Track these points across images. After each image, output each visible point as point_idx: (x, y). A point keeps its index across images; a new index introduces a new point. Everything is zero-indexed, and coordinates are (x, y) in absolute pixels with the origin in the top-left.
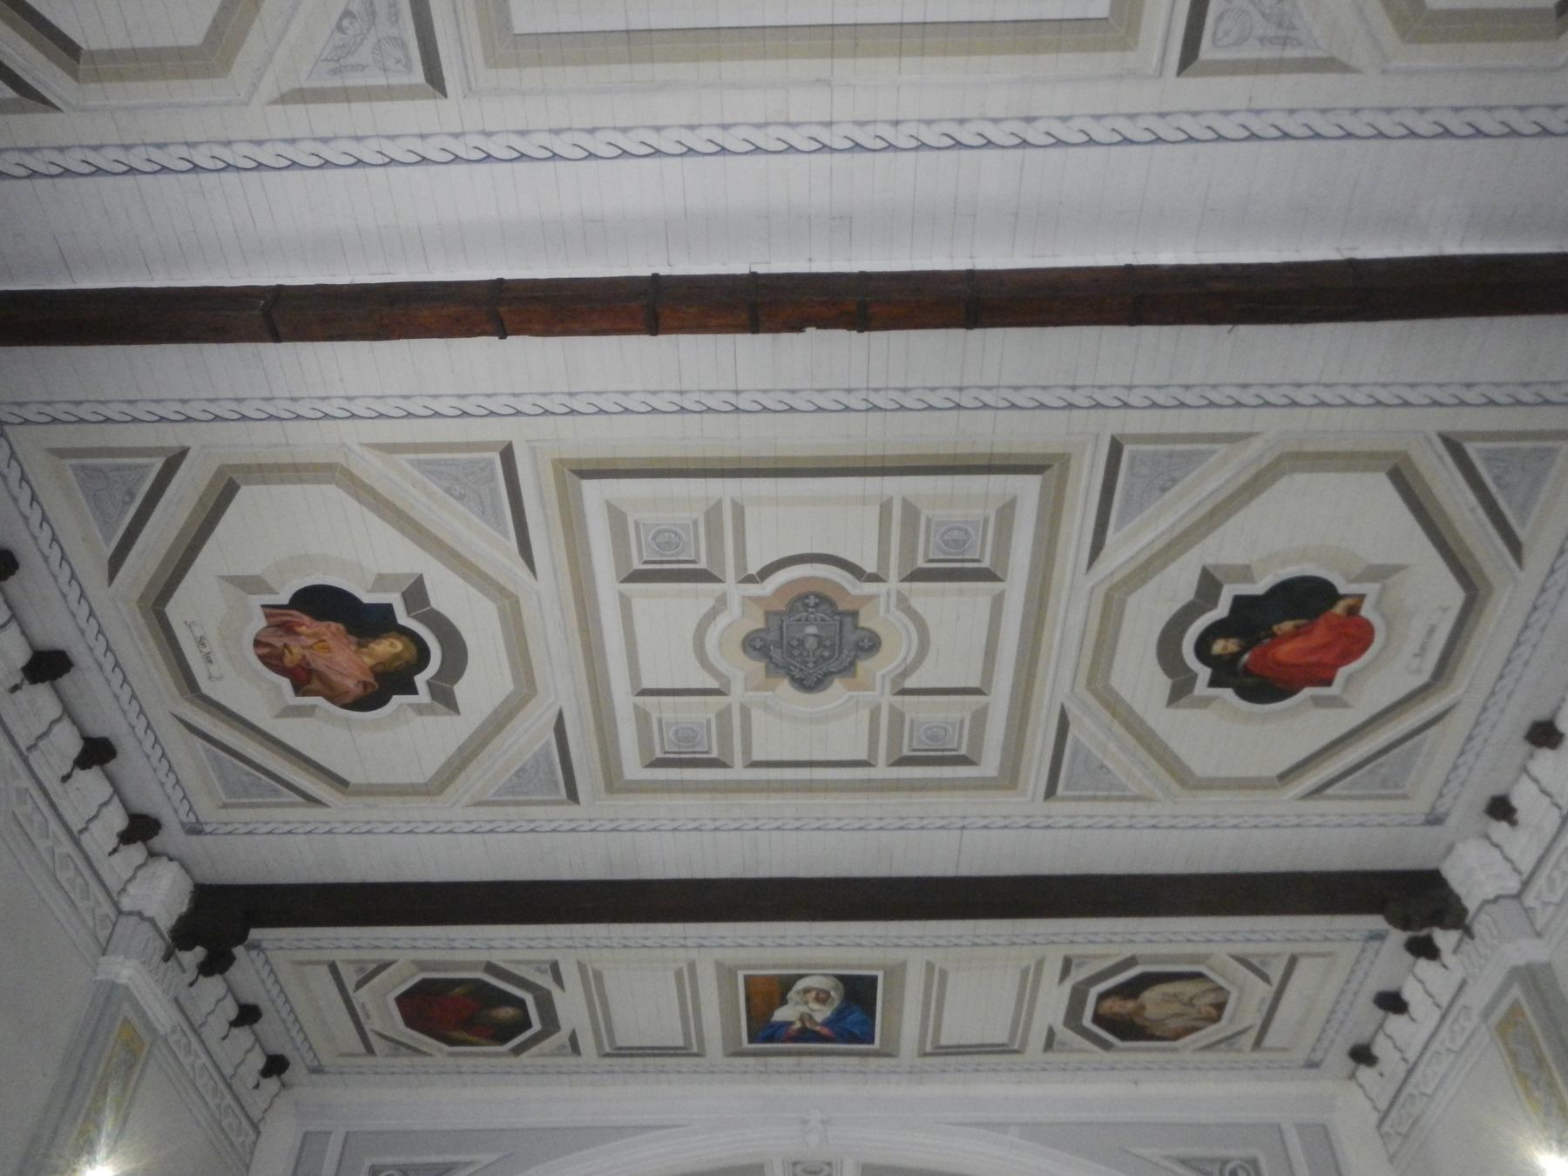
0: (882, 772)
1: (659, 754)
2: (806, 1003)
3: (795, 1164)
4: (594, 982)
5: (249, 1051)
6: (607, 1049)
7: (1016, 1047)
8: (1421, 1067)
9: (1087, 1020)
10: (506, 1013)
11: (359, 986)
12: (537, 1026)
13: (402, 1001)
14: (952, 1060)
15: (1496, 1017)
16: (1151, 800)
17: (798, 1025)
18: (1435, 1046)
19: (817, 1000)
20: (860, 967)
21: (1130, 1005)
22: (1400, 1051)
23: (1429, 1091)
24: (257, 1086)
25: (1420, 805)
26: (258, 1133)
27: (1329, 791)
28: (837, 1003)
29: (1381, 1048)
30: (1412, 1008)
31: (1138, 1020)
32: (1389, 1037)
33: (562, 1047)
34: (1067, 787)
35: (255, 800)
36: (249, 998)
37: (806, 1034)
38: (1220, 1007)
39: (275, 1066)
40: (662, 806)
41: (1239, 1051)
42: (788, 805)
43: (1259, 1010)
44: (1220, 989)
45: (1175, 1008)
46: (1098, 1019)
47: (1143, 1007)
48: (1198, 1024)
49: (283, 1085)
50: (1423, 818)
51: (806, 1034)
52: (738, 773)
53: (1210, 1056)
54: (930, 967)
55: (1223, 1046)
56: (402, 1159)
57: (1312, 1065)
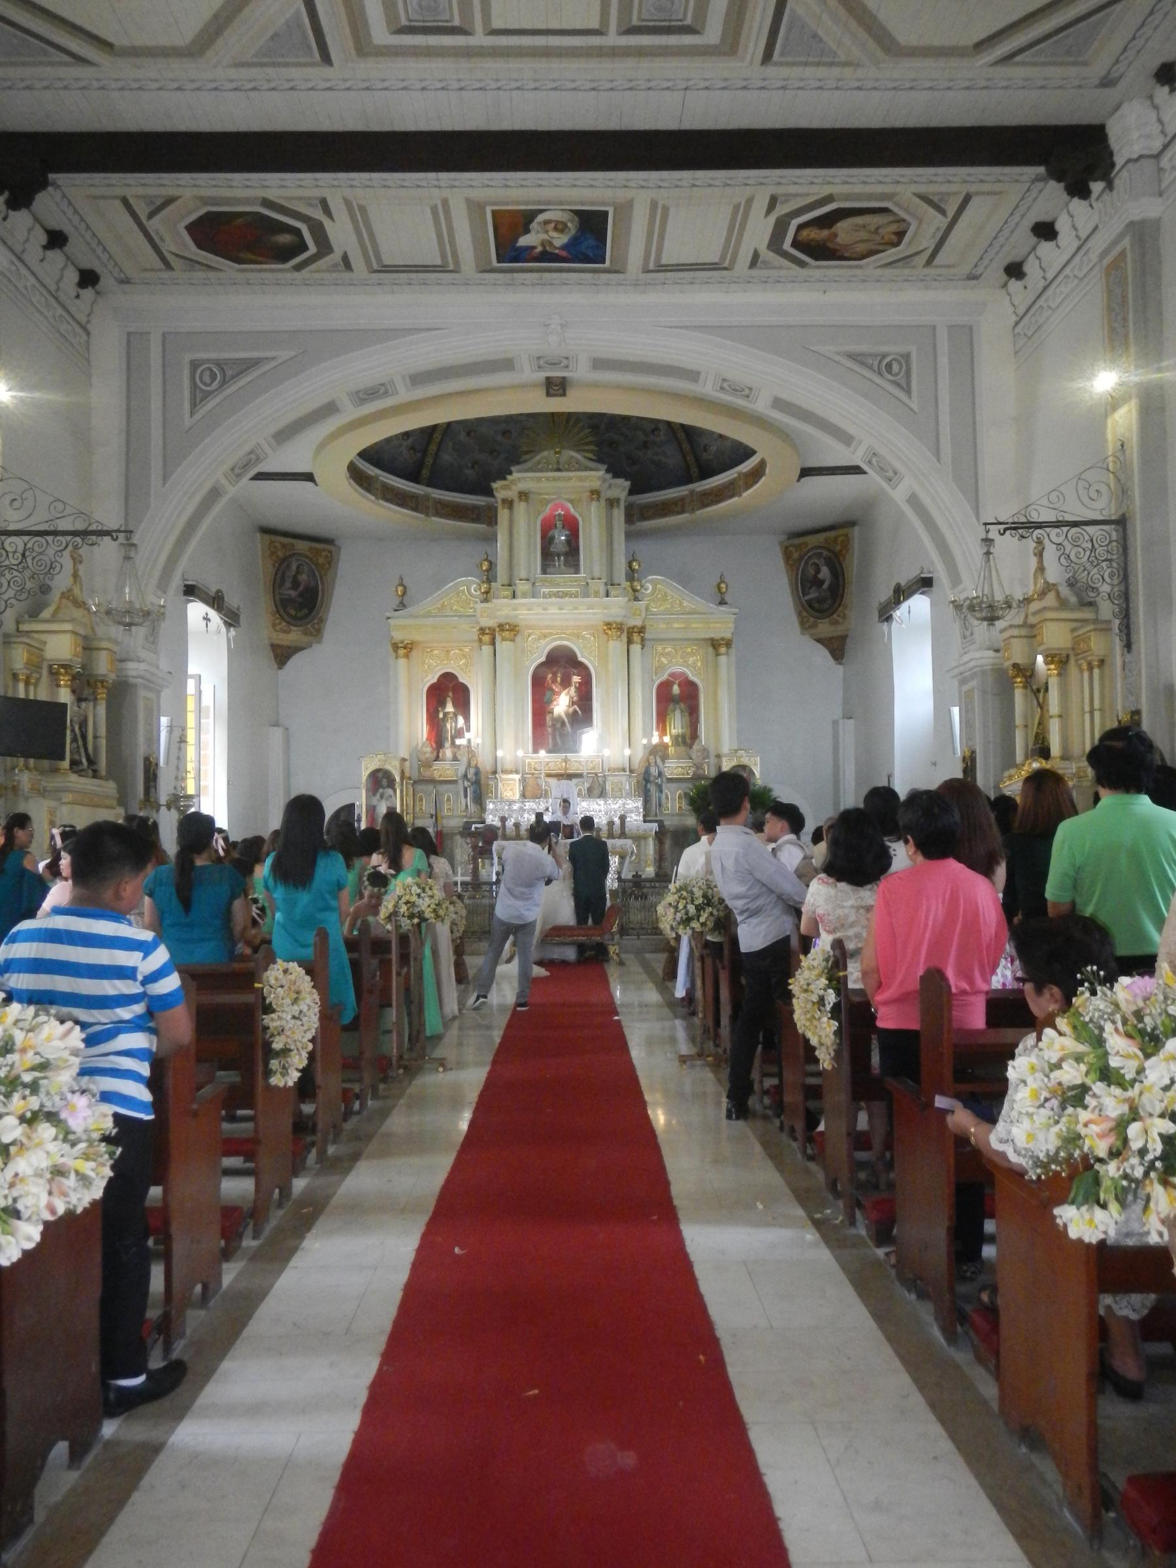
0: (613, 39)
1: (404, 22)
2: (547, 232)
3: (539, 358)
4: (359, 215)
5: (63, 269)
6: (375, 266)
7: (726, 264)
8: (1054, 286)
9: (787, 245)
10: (285, 239)
11: (151, 215)
12: (312, 249)
13: (190, 228)
14: (669, 274)
15: (1106, 262)
16: (858, 65)
17: (540, 249)
18: (1067, 271)
19: (556, 229)
20: (592, 204)
21: (825, 233)
22: (1044, 270)
23: (1053, 306)
24: (78, 296)
25: (1098, 69)
26: (88, 334)
27: (1018, 59)
28: (573, 232)
29: (1030, 267)
30: (1060, 237)
31: (830, 245)
32: (1038, 258)
33: (336, 265)
34: (782, 54)
35: (28, 59)
36: (54, 225)
37: (547, 256)
38: (901, 235)
39: (88, 279)
40: (412, 68)
41: (914, 267)
42: (526, 68)
43: (933, 237)
44: (904, 220)
45: (863, 235)
46: (796, 244)
47: (835, 235)
48: (881, 248)
49: (98, 293)
50: (1097, 82)
51: (547, 256)
52: (479, 39)
53: (888, 272)
54: (654, 205)
55: (900, 264)
56: (214, 355)
57: (972, 277)
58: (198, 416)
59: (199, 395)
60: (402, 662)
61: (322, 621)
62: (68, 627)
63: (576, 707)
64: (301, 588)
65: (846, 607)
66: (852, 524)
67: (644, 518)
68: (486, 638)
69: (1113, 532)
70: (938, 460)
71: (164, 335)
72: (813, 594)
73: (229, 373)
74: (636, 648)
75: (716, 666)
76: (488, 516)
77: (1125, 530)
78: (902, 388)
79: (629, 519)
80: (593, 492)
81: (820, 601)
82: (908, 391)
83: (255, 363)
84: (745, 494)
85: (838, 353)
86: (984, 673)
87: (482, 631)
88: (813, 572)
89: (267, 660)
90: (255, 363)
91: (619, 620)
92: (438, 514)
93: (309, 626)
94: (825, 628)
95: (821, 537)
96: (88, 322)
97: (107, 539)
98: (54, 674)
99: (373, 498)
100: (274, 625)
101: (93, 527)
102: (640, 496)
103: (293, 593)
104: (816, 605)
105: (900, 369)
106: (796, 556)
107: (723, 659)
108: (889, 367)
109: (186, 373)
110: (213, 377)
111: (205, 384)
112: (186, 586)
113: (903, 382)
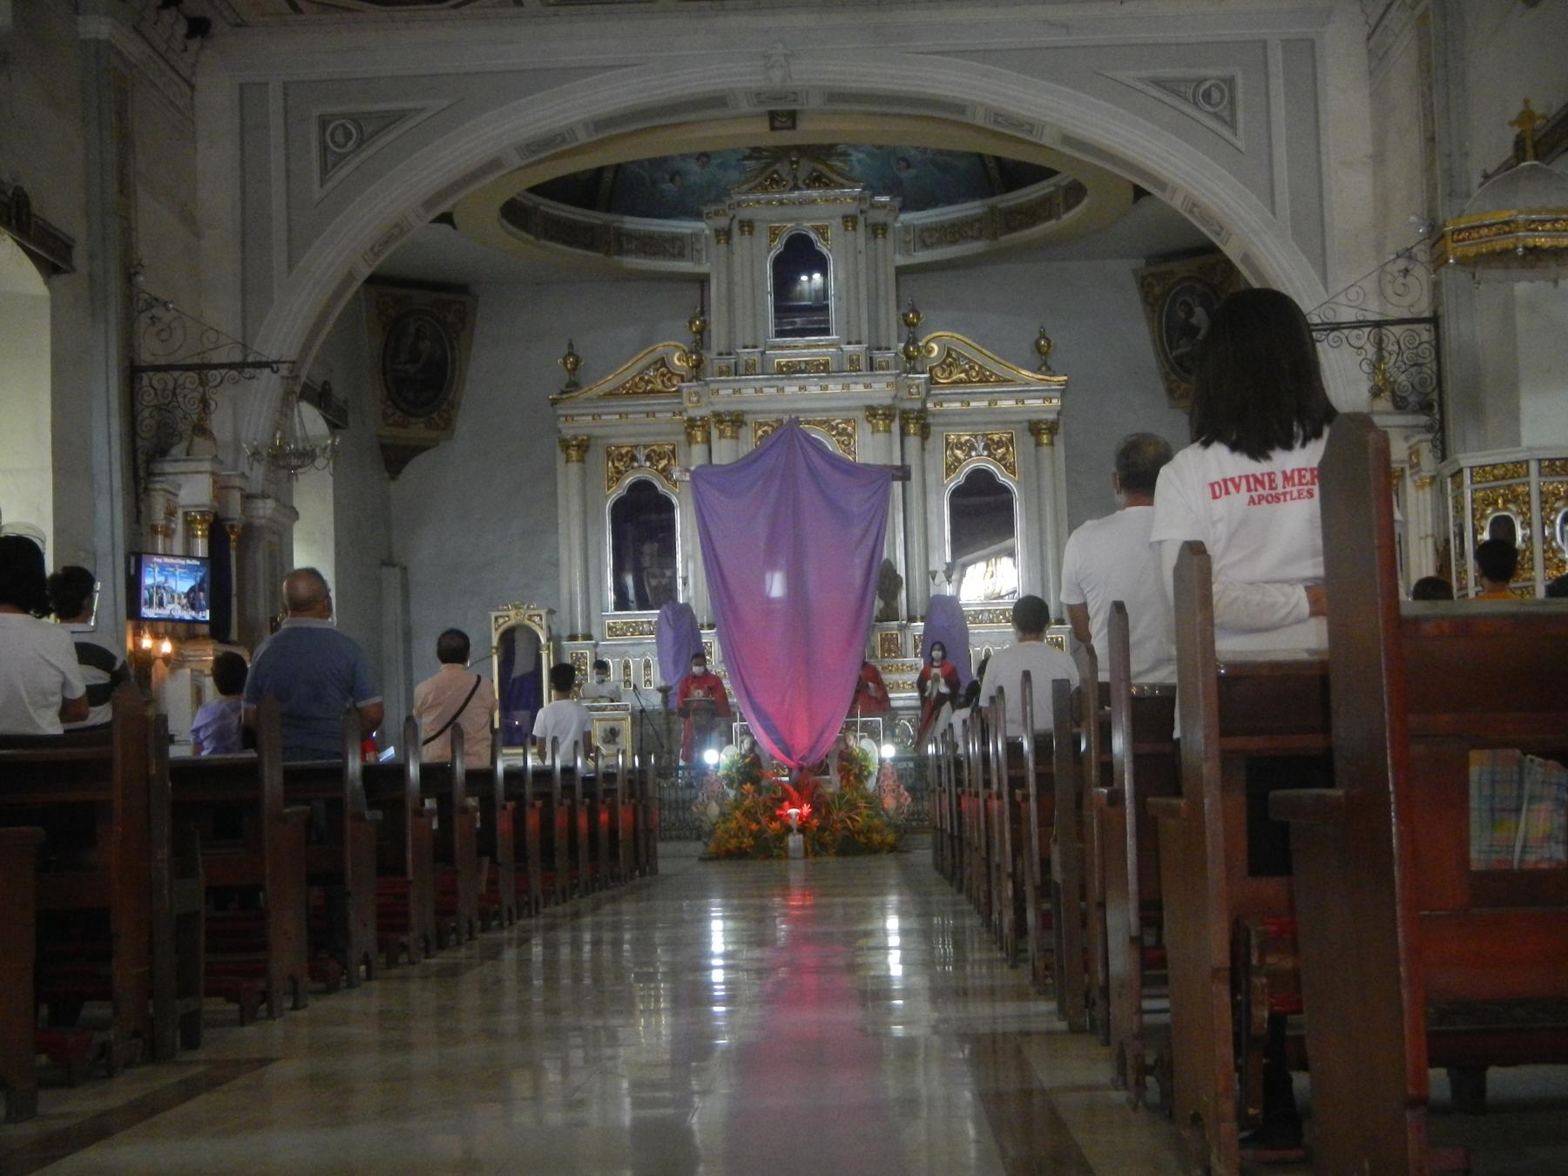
26: (192, 87)
56: (351, 108)
58: (329, 185)
59: (331, 159)
60: (574, 467)
62: (207, 466)
68: (699, 435)
69: (1425, 333)
70: (1274, 213)
71: (286, 86)
73: (368, 129)
74: (913, 442)
75: (1038, 462)
77: (1437, 328)
78: (1225, 122)
80: (846, 218)
82: (1232, 125)
83: (401, 116)
85: (1141, 80)
87: (691, 423)
88: (1183, 315)
90: (401, 116)
91: (889, 402)
93: (435, 415)
96: (194, 74)
97: (267, 371)
98: (189, 524)
99: (531, 238)
100: (385, 416)
106: (1157, 290)
107: (1046, 450)
108: (1207, 95)
109: (314, 129)
110: (348, 136)
111: (339, 146)
113: (1226, 114)
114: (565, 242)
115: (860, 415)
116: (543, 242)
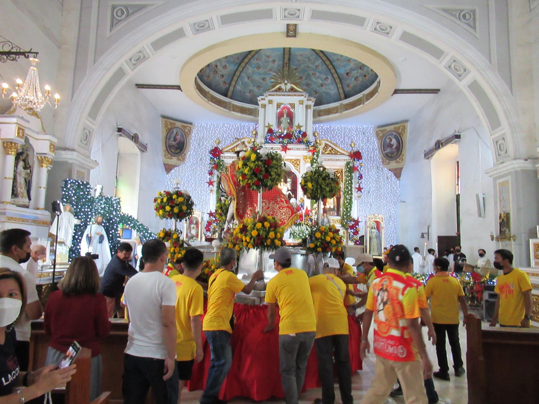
58: (113, 32)
59: (115, 22)
61: (185, 155)
63: (290, 192)
64: (177, 141)
65: (403, 156)
66: (406, 121)
67: (320, 115)
70: (490, 62)
72: (388, 150)
73: (130, 11)
76: (254, 113)
78: (471, 26)
79: (314, 116)
80: (300, 101)
81: (392, 153)
82: (474, 28)
84: (366, 103)
86: (516, 172)
89: (162, 170)
92: (234, 110)
94: (393, 164)
95: (392, 127)
97: (22, 57)
100: (165, 156)
101: (14, 50)
102: (319, 107)
103: (174, 143)
104: (390, 155)
105: (470, 17)
106: (381, 135)
108: (464, 16)
110: (123, 13)
112: (118, 128)
113: (472, 24)
114: (217, 105)
115: (301, 159)
116: (210, 103)
